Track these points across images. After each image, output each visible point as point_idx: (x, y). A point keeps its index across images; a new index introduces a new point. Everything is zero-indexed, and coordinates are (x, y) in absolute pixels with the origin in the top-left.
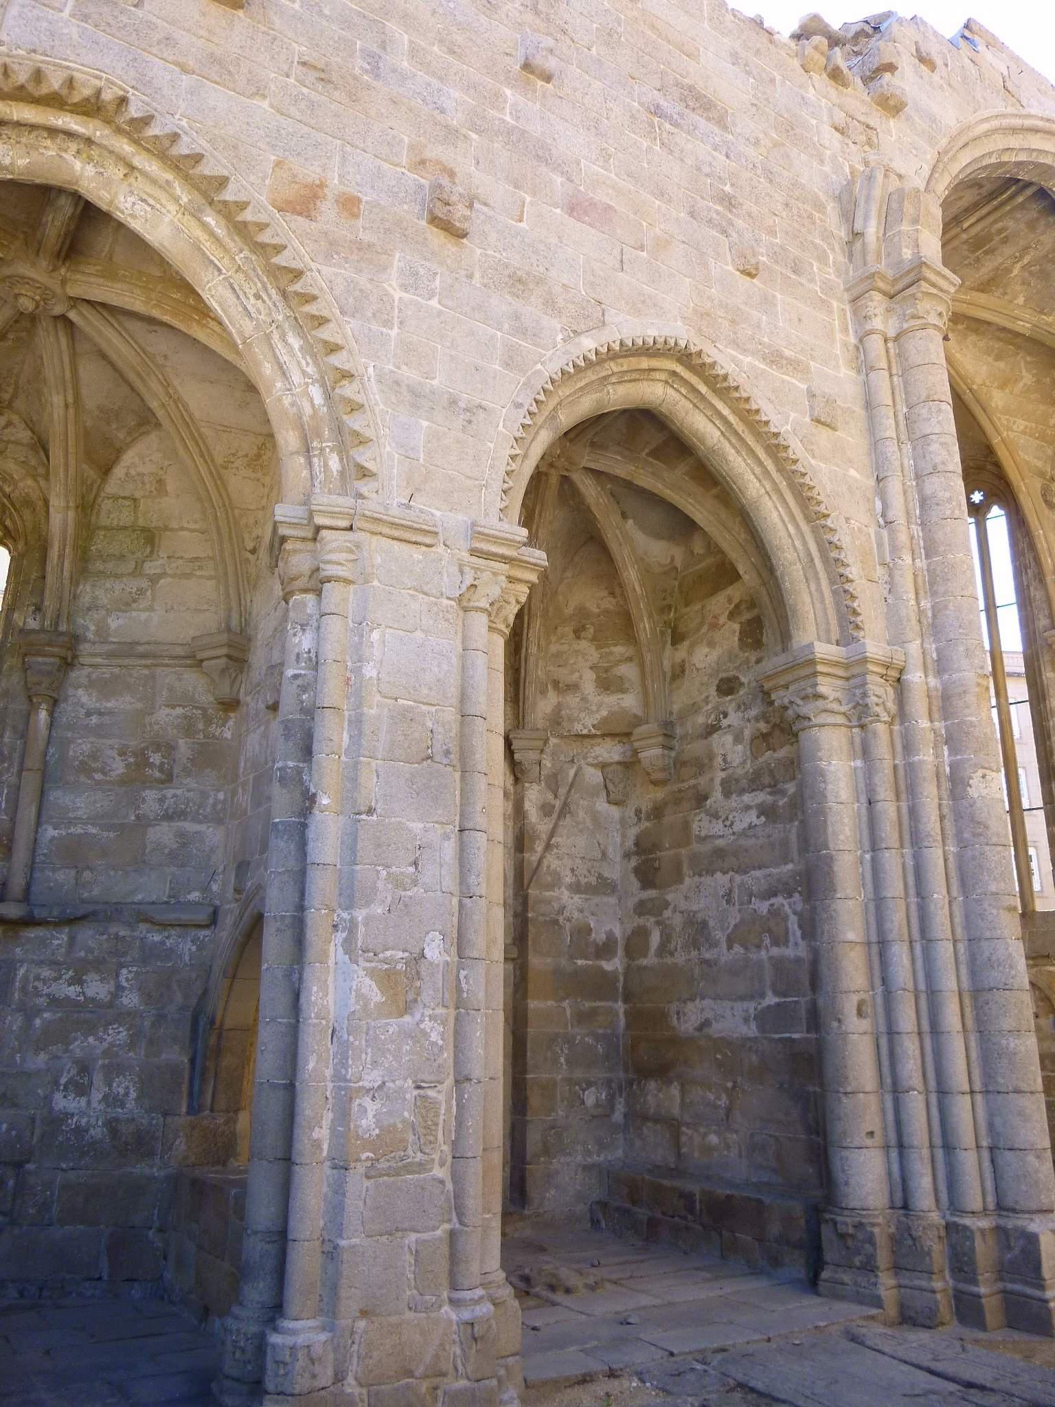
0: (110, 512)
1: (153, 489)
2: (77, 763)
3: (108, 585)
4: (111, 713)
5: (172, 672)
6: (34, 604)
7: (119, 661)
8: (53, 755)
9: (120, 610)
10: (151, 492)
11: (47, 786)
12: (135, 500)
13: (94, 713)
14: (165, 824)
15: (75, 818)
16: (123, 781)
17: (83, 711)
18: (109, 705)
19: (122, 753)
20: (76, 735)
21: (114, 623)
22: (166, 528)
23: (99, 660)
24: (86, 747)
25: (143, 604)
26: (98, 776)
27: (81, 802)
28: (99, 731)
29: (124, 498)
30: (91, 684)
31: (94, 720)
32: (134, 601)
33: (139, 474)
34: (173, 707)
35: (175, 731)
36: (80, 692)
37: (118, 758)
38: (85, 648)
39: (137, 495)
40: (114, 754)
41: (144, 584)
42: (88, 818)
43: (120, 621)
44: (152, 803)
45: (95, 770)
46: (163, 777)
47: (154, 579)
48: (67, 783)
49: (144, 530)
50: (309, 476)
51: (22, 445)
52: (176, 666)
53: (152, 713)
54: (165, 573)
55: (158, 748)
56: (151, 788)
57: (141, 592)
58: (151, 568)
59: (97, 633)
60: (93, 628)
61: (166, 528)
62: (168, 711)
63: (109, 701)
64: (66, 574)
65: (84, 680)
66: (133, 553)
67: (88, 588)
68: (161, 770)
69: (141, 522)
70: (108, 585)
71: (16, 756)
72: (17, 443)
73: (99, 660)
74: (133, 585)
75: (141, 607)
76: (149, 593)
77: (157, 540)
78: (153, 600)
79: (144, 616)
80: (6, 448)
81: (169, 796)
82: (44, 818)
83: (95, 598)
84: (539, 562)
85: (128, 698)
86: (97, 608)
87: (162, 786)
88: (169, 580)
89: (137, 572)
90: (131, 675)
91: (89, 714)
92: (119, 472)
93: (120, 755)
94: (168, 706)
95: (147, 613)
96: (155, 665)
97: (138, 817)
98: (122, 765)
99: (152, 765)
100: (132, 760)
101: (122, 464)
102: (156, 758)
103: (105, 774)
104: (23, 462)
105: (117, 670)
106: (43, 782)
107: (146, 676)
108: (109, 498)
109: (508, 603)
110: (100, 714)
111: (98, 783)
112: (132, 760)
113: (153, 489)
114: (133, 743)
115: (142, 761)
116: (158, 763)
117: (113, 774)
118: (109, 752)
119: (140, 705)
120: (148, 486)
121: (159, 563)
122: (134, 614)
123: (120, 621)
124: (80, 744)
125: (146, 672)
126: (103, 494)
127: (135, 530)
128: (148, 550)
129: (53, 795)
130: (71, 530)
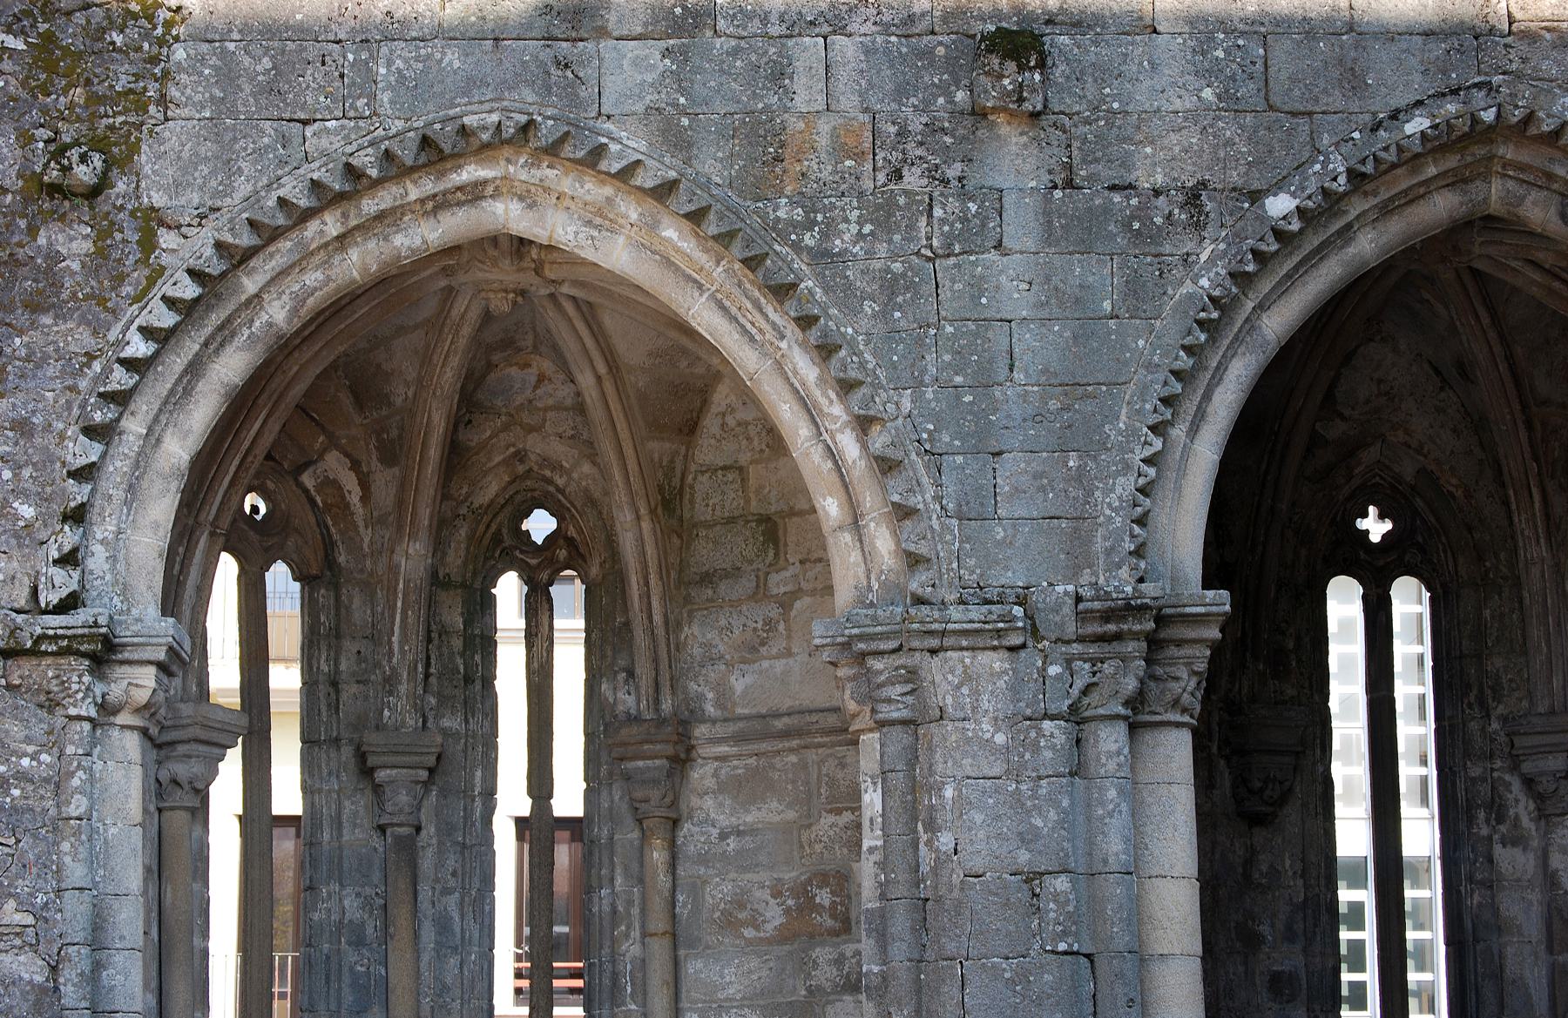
0: (707, 497)
1: (764, 447)
2: (718, 914)
3: (723, 622)
4: (752, 831)
5: (831, 755)
6: (624, 670)
7: (755, 747)
8: (685, 905)
9: (744, 661)
10: (762, 451)
11: (682, 952)
12: (741, 469)
13: (731, 833)
14: (848, 998)
15: (727, 999)
16: (784, 936)
17: (715, 832)
18: (749, 819)
19: (776, 894)
20: (711, 872)
21: (739, 684)
22: (793, 513)
23: (724, 749)
24: (727, 888)
25: (777, 645)
26: (749, 933)
27: (729, 974)
28: (744, 862)
29: (724, 468)
30: (722, 788)
31: (732, 844)
32: (763, 644)
33: (739, 424)
34: (838, 812)
35: (845, 851)
36: (709, 802)
37: (772, 901)
38: (701, 731)
39: (744, 459)
40: (765, 894)
41: (774, 612)
42: (743, 998)
43: (749, 679)
44: (827, 968)
45: (744, 924)
46: (837, 925)
47: (786, 603)
48: (708, 947)
49: (764, 520)
50: (860, 559)
51: (566, 409)
52: (833, 745)
53: (809, 826)
54: (800, 589)
55: (823, 879)
56: (822, 944)
57: (770, 625)
58: (779, 583)
59: (719, 704)
60: (710, 695)
61: (793, 513)
62: (831, 819)
63: (748, 811)
64: (658, 618)
65: (710, 783)
66: (751, 562)
67: (696, 629)
68: (833, 916)
69: (755, 507)
70: (723, 622)
71: (635, 911)
72: (558, 407)
73: (724, 749)
74: (757, 614)
75: (774, 651)
76: (781, 627)
77: (781, 533)
78: (789, 637)
79: (780, 665)
80: (545, 420)
81: (849, 954)
82: (684, 1004)
83: (708, 646)
84: (1214, 609)
85: (774, 804)
86: (713, 661)
87: (835, 939)
88: (807, 600)
89: (760, 593)
90: (772, 767)
91: (723, 836)
92: (711, 424)
93: (774, 896)
94: (830, 811)
95: (784, 661)
96: (806, 747)
97: (809, 990)
98: (779, 910)
99: (819, 908)
100: (790, 902)
101: (714, 409)
102: (824, 897)
103: (757, 928)
104: (573, 437)
105: (752, 761)
106: (675, 947)
107: (793, 764)
108: (703, 473)
109: (1177, 679)
110: (739, 833)
111: (749, 942)
112: (790, 902)
113: (764, 447)
114: (789, 876)
115: (807, 905)
116: (827, 903)
117: (769, 927)
118: (758, 894)
119: (791, 815)
120: (756, 443)
121: (787, 574)
122: (766, 664)
123: (749, 679)
124: (718, 884)
125: (793, 758)
126: (693, 468)
127: (747, 522)
128: (771, 553)
129: (693, 967)
130: (650, 550)
